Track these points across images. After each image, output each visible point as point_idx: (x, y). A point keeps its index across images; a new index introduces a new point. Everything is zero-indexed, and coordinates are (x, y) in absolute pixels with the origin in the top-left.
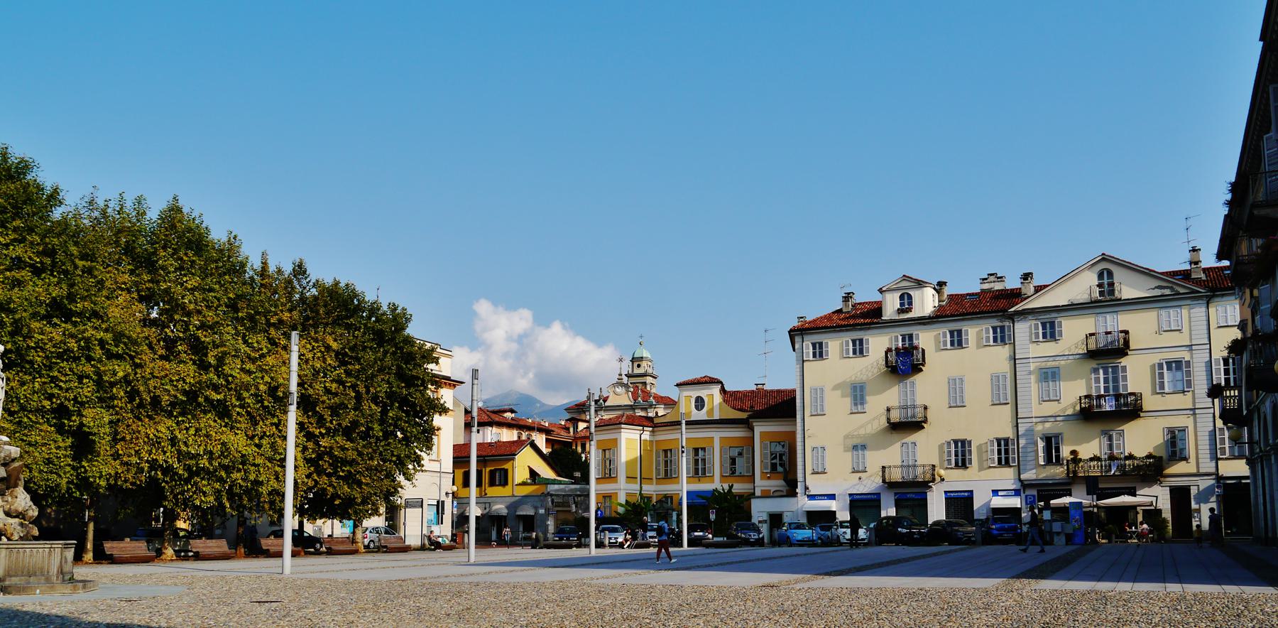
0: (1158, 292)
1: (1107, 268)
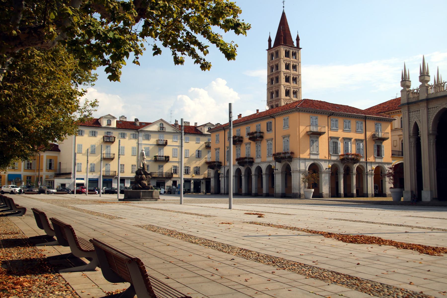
0: (173, 131)
1: (162, 123)
